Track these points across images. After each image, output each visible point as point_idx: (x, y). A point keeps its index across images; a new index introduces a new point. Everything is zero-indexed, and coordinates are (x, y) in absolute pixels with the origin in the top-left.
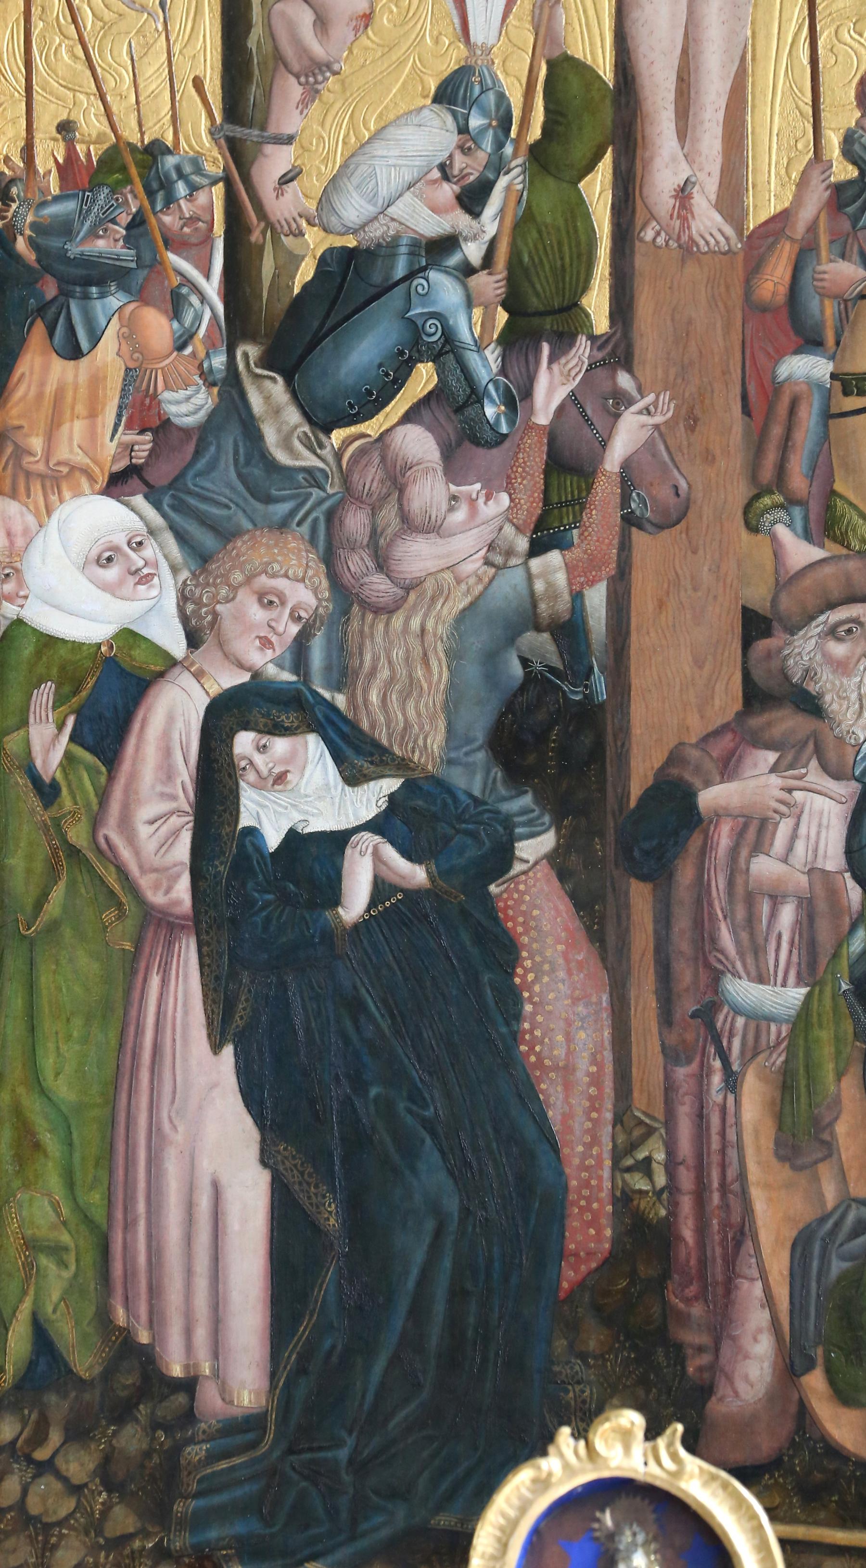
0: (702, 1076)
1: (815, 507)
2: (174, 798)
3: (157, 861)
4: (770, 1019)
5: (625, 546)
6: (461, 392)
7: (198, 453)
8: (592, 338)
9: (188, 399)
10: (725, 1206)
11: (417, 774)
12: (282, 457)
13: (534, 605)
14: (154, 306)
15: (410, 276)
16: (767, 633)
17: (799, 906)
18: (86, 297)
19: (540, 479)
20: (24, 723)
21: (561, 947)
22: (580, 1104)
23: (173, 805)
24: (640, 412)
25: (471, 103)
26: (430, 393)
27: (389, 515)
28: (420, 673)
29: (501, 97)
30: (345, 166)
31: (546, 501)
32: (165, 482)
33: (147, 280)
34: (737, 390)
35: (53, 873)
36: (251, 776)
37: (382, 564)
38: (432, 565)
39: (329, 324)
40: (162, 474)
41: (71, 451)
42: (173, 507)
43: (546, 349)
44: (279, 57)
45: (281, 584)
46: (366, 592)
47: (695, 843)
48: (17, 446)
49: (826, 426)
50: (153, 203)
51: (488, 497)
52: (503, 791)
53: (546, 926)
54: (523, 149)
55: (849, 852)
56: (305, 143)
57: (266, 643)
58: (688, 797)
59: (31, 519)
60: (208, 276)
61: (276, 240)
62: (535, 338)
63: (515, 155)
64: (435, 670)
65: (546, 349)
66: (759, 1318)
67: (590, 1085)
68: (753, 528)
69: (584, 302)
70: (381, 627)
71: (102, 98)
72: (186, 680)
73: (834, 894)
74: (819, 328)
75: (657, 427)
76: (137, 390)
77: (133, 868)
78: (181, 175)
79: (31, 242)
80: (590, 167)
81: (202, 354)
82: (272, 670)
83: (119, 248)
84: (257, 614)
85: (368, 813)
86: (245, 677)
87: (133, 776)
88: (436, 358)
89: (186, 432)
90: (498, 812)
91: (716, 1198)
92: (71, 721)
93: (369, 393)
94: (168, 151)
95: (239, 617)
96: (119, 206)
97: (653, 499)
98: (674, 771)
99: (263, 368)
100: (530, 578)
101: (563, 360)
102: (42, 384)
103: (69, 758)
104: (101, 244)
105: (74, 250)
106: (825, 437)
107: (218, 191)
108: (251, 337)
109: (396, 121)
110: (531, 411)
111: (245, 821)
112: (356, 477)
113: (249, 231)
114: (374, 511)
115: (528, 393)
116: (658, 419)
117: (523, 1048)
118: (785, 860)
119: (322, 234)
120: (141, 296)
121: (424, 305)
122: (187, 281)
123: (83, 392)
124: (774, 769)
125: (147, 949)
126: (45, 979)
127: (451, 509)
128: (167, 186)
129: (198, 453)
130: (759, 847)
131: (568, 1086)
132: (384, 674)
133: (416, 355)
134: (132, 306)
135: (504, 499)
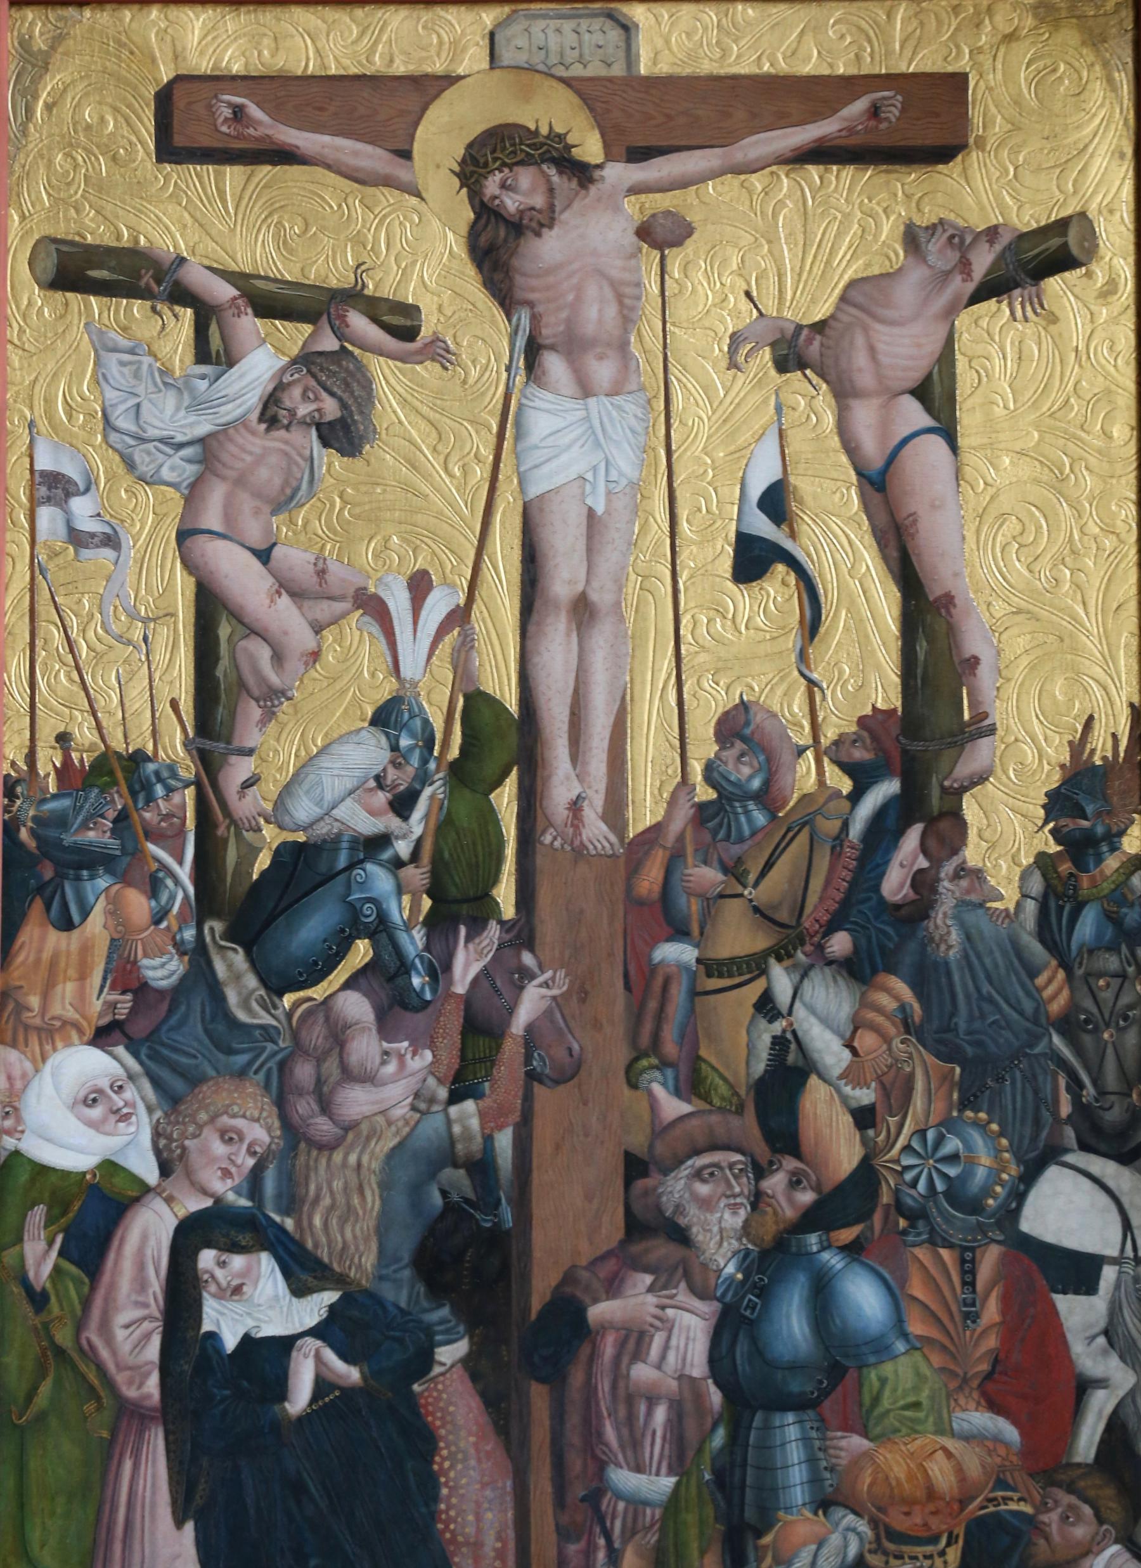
1: (684, 1069)
2: (146, 1305)
3: (131, 1361)
4: (646, 1503)
5: (528, 1098)
6: (392, 965)
7: (171, 1012)
8: (501, 922)
9: (163, 965)
11: (353, 1288)
12: (242, 1016)
14: (135, 887)
15: (351, 867)
16: (645, 1174)
17: (670, 1408)
18: (78, 878)
19: (458, 1038)
20: (20, 1240)
21: (472, 1439)
23: (145, 1312)
24: (540, 986)
25: (401, 727)
26: (367, 965)
27: (331, 1067)
28: (356, 1201)
29: (426, 722)
30: (296, 774)
31: (463, 1058)
32: (144, 1035)
33: (129, 865)
34: (620, 969)
35: (41, 1372)
36: (213, 1288)
37: (326, 1106)
38: (367, 1110)
39: (283, 905)
40: (140, 1028)
41: (64, 1008)
42: (149, 1057)
43: (463, 930)
44: (242, 685)
45: (239, 1123)
46: (311, 1131)
47: (585, 1351)
48: (17, 1003)
49: (692, 1002)
50: (135, 802)
51: (414, 1054)
52: (425, 1304)
53: (460, 1420)
54: (444, 765)
55: (713, 1360)
56: (263, 755)
57: (226, 1174)
58: (580, 1313)
59: (28, 1065)
60: (181, 863)
61: (238, 835)
62: (454, 922)
63: (438, 771)
64: (369, 1199)
65: (463, 930)
67: (496, 1558)
68: (633, 1085)
69: (494, 892)
70: (324, 1161)
71: (94, 714)
72: (158, 1204)
73: (699, 1397)
75: (554, 998)
76: (120, 957)
77: (111, 1367)
78: (160, 780)
79: (32, 832)
80: (499, 782)
81: (175, 928)
82: (231, 1197)
83: (107, 839)
84: (219, 1148)
85: (311, 1321)
86: (208, 1203)
87: (113, 1286)
88: (371, 935)
89: (161, 992)
90: (420, 1322)
92: (59, 1239)
93: (316, 963)
94: (148, 759)
95: (205, 1150)
96: (107, 803)
97: (552, 1059)
98: (568, 1290)
99: (227, 940)
100: (449, 1122)
101: (477, 941)
102: (40, 951)
103: (57, 1270)
104: (91, 835)
105: (69, 839)
106: (692, 1011)
107: (190, 794)
108: (217, 915)
109: (341, 739)
110: (450, 982)
111: (207, 1326)
112: (304, 1033)
113: (216, 826)
114: (319, 1061)
115: (448, 967)
116: (555, 992)
117: (440, 1526)
118: (659, 1367)
119: (277, 830)
120: (125, 879)
121: (362, 892)
122: (164, 867)
123: (74, 958)
124: (651, 1289)
125: (121, 1438)
126: (33, 1464)
127: (384, 1063)
128: (147, 788)
129: (171, 1012)
130: (639, 1355)
132: (327, 1201)
133: (355, 933)
134: (117, 887)
135: (428, 1055)
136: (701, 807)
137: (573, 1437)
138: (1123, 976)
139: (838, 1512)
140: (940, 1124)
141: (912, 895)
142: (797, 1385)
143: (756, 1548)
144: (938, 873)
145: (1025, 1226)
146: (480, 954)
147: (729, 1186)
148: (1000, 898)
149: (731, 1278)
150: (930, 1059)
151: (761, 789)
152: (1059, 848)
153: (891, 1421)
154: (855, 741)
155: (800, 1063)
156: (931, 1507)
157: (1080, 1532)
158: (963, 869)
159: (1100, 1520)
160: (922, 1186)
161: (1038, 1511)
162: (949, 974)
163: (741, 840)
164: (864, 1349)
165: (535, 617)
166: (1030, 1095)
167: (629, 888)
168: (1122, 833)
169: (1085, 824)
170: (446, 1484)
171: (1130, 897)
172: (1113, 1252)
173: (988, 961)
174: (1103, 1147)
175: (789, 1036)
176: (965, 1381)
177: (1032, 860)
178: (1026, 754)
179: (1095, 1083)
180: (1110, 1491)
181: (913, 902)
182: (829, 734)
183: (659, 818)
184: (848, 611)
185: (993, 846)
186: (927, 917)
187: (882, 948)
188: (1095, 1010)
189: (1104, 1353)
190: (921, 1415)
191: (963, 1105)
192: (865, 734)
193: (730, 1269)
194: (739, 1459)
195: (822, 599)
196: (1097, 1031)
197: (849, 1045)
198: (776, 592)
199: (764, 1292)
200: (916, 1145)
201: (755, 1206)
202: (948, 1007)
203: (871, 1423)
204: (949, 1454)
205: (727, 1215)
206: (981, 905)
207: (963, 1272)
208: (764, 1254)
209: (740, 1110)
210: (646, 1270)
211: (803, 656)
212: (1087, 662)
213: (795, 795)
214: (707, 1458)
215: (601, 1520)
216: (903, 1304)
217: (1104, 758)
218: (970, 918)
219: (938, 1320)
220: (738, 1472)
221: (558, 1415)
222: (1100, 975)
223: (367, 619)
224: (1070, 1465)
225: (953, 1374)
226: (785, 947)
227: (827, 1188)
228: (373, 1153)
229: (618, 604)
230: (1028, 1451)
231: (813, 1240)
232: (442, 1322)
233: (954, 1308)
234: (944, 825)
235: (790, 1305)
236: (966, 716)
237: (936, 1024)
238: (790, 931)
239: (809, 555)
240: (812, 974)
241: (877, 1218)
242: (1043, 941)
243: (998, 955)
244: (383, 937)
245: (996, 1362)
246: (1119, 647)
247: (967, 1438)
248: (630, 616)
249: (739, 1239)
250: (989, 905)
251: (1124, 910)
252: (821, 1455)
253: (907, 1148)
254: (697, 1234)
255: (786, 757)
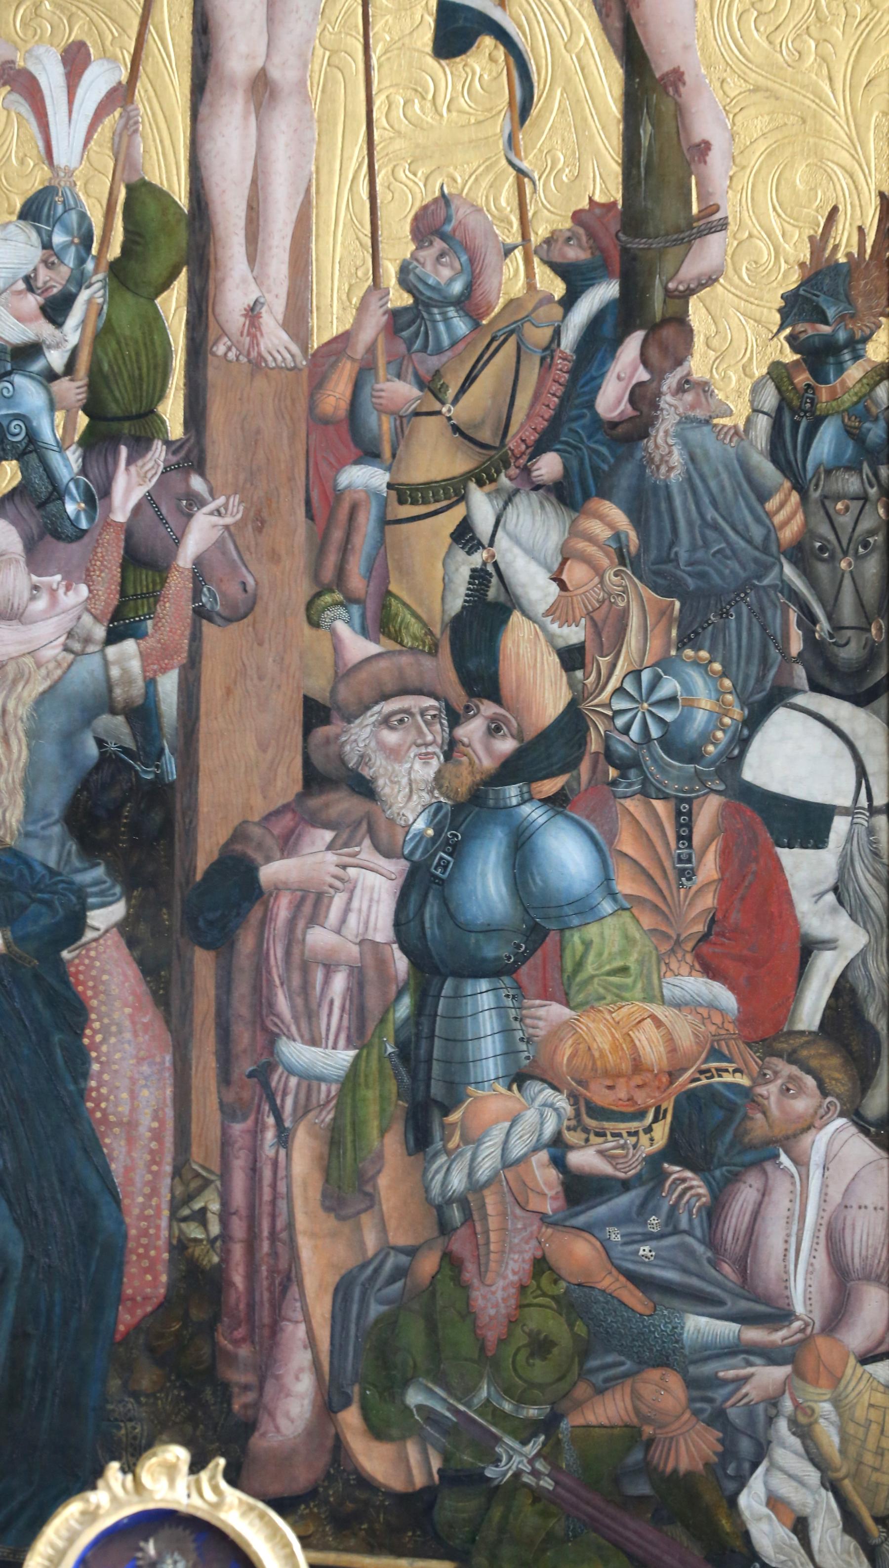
0: (257, 1132)
1: (372, 606)
4: (321, 1079)
5: (196, 637)
8: (167, 443)
10: (274, 1254)
13: (110, 689)
16: (326, 721)
17: (350, 975)
19: (117, 572)
21: (128, 1010)
22: (141, 1157)
26: (14, 490)
29: (83, 216)
31: (123, 593)
34: (301, 496)
38: (13, 650)
43: (124, 451)
47: (256, 913)
49: (382, 531)
51: (68, 588)
52: (77, 863)
53: (115, 990)
54: (104, 265)
55: (398, 924)
58: (250, 871)
62: (114, 440)
63: (96, 271)
65: (124, 451)
66: (301, 1358)
67: (152, 1139)
68: (315, 624)
69: (160, 409)
73: (383, 964)
74: (377, 441)
75: (227, 527)
80: (166, 285)
88: (20, 456)
90: (71, 883)
91: (266, 1246)
97: (223, 594)
98: (238, 847)
100: (106, 664)
106: (381, 542)
110: (109, 509)
115: (106, 493)
116: (228, 520)
117: (90, 1105)
118: (338, 932)
121: (9, 407)
124: (330, 847)
127: (33, 598)
130: (314, 920)
131: (131, 1141)
135: (83, 590)
136: (395, 314)
137: (241, 1006)
138: (864, 498)
139: (534, 1087)
140: (657, 664)
141: (630, 412)
142: (491, 950)
143: (443, 1126)
144: (660, 386)
145: (749, 774)
146: (144, 478)
147: (420, 733)
148: (730, 413)
149: (421, 835)
150: (647, 593)
151: (462, 294)
152: (797, 357)
153: (596, 987)
154: (569, 239)
155: (502, 598)
156: (637, 1080)
157: (801, 1105)
158: (687, 382)
159: (824, 1092)
160: (635, 732)
161: (755, 1083)
162: (669, 499)
163: (439, 351)
164: (568, 910)
165: (208, 96)
166: (757, 632)
167: (312, 407)
168: (866, 339)
169: (825, 329)
170: (97, 1059)
171: (874, 410)
172: (847, 802)
173: (713, 484)
174: (837, 687)
175: (490, 568)
176: (678, 943)
177: (765, 371)
178: (760, 252)
179: (829, 618)
180: (835, 1061)
181: (631, 419)
182: (540, 232)
183: (348, 327)
184: (564, 90)
185: (721, 356)
186: (647, 435)
187: (595, 470)
188: (832, 537)
189: (833, 911)
190: (629, 981)
191: (682, 644)
192: (581, 231)
193: (420, 824)
194: (426, 1030)
195: (535, 77)
196: (832, 558)
197: (557, 579)
198: (483, 69)
199: (456, 849)
200: (629, 686)
201: (448, 756)
202: (669, 534)
203: (574, 989)
204: (658, 1023)
205: (417, 765)
206: (707, 422)
207: (679, 826)
208: (458, 808)
209: (434, 651)
210: (327, 825)
211: (511, 142)
212: (832, 147)
213: (501, 300)
214: (390, 1029)
215: (271, 1097)
216: (611, 862)
217: (849, 255)
218: (696, 435)
219: (650, 878)
220: (424, 1044)
221: (225, 984)
222: (838, 498)
223: (15, 97)
224: (792, 1033)
225: (666, 936)
226: (487, 470)
227: (531, 733)
228: (19, 698)
229: (302, 83)
230: (745, 1020)
231: (512, 792)
232: (97, 883)
233: (668, 865)
234: (668, 333)
235: (485, 863)
236: (695, 209)
237: (653, 554)
238: (492, 453)
239: (520, 27)
240: (517, 499)
241: (585, 767)
242: (775, 461)
243: (725, 476)
244: (33, 459)
245: (713, 921)
246: (868, 128)
247: (678, 1005)
248: (316, 95)
249: (431, 792)
250: (715, 421)
251: (867, 425)
252: (517, 1025)
253: (620, 690)
254: (383, 786)
255: (492, 257)
